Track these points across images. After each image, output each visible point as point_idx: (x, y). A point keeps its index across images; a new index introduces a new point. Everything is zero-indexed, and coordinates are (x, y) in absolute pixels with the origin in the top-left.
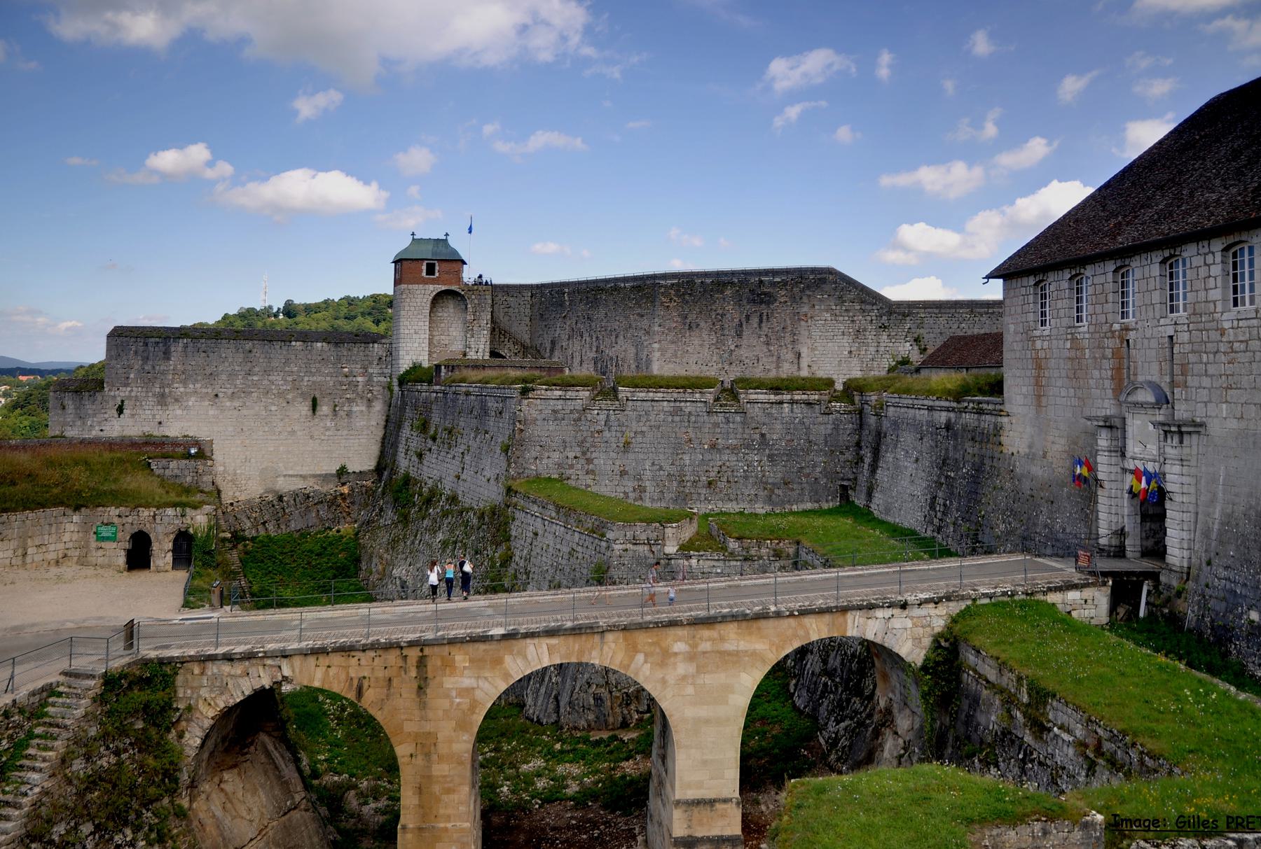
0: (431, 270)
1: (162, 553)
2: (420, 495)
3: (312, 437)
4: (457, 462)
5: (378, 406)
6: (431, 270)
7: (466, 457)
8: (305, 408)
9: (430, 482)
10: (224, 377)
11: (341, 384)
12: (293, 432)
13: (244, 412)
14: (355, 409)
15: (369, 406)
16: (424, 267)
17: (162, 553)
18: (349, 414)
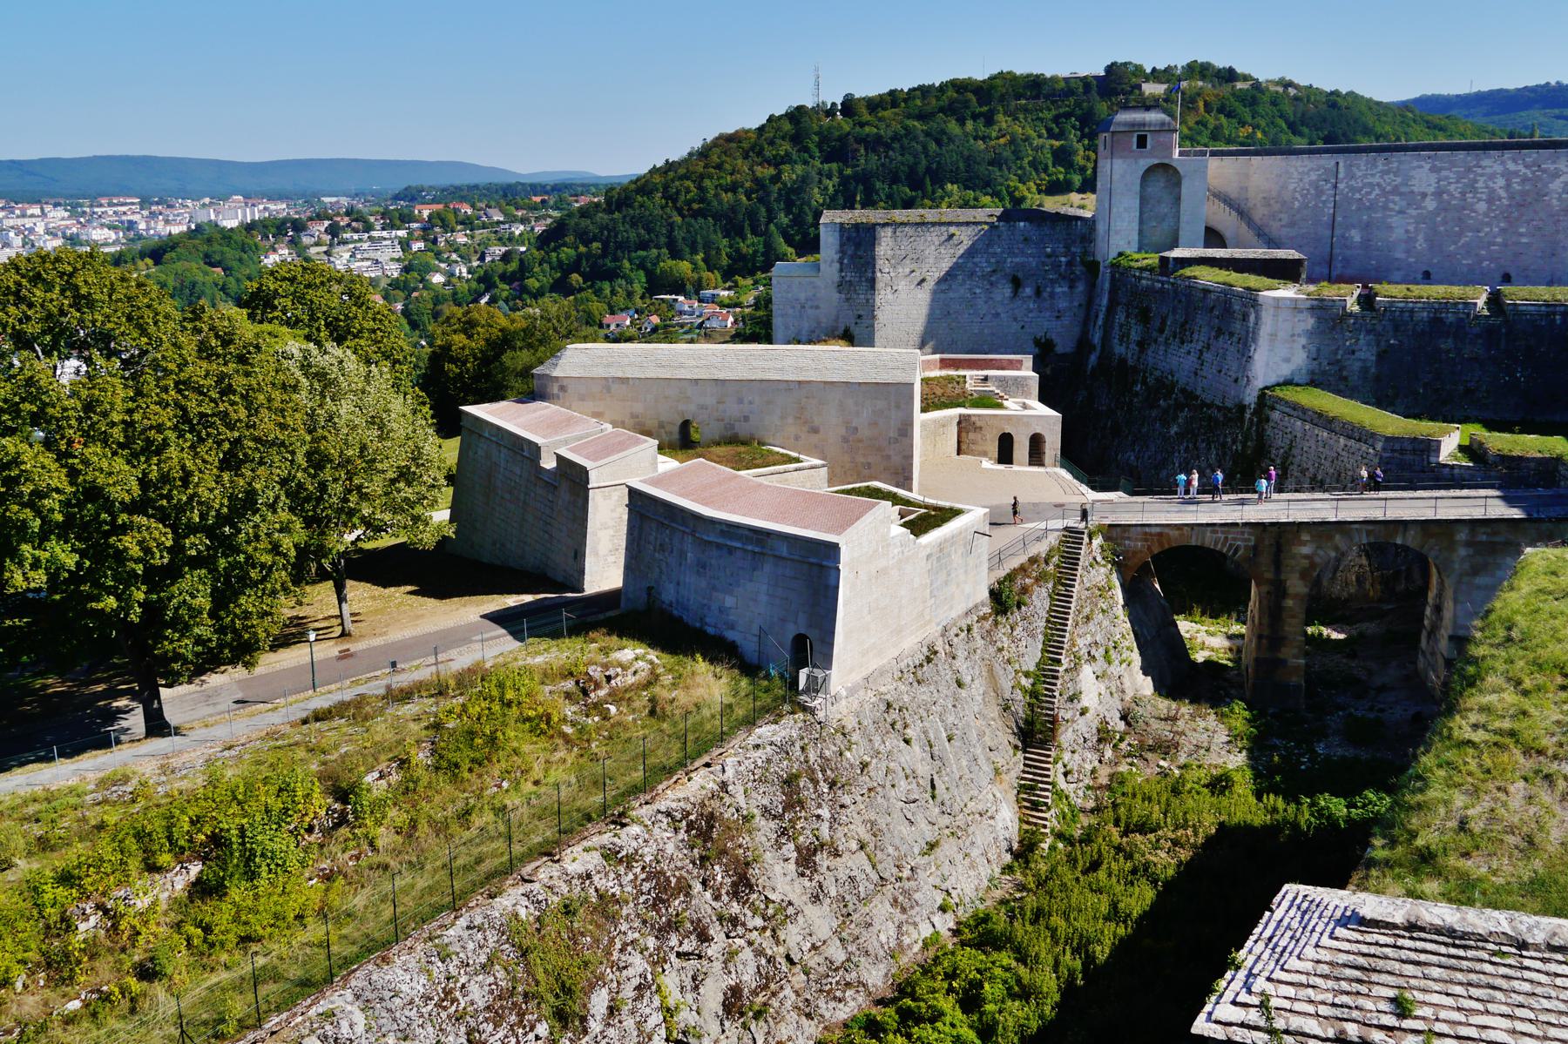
0: (1142, 142)
1: (1021, 449)
2: (1144, 383)
3: (1015, 319)
4: (1193, 358)
5: (1080, 287)
6: (1142, 142)
7: (1207, 356)
8: (1008, 291)
9: (1158, 373)
10: (931, 261)
11: (1044, 264)
12: (997, 315)
13: (951, 295)
14: (1058, 290)
15: (1071, 287)
16: (1135, 140)
17: (1021, 449)
18: (1052, 295)
